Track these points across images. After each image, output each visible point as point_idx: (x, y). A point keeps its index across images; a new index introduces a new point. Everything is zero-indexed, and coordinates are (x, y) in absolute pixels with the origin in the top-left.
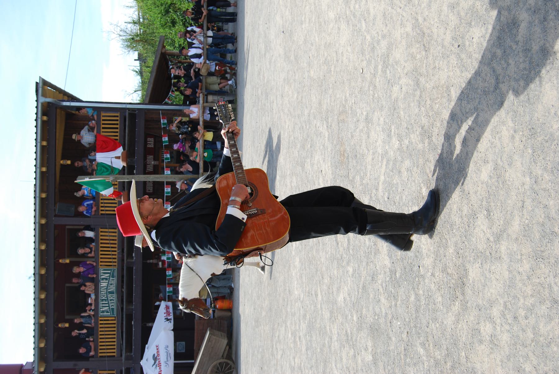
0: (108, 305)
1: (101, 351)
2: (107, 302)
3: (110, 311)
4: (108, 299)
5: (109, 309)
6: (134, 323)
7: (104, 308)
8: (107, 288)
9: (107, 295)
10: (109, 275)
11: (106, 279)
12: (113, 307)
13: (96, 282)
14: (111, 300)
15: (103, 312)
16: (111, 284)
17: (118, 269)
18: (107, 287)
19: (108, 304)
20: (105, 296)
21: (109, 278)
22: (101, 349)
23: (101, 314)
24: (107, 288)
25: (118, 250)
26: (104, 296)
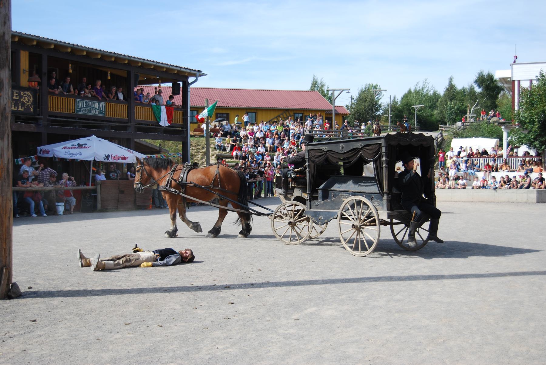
1: (59, 98)
3: (79, 108)
4: (86, 107)
5: (80, 108)
6: (71, 128)
7: (81, 103)
8: (93, 107)
9: (88, 107)
11: (99, 107)
13: (94, 98)
14: (86, 110)
15: (79, 102)
16: (96, 111)
19: (84, 108)
21: (99, 110)
22: (63, 98)
24: (93, 107)
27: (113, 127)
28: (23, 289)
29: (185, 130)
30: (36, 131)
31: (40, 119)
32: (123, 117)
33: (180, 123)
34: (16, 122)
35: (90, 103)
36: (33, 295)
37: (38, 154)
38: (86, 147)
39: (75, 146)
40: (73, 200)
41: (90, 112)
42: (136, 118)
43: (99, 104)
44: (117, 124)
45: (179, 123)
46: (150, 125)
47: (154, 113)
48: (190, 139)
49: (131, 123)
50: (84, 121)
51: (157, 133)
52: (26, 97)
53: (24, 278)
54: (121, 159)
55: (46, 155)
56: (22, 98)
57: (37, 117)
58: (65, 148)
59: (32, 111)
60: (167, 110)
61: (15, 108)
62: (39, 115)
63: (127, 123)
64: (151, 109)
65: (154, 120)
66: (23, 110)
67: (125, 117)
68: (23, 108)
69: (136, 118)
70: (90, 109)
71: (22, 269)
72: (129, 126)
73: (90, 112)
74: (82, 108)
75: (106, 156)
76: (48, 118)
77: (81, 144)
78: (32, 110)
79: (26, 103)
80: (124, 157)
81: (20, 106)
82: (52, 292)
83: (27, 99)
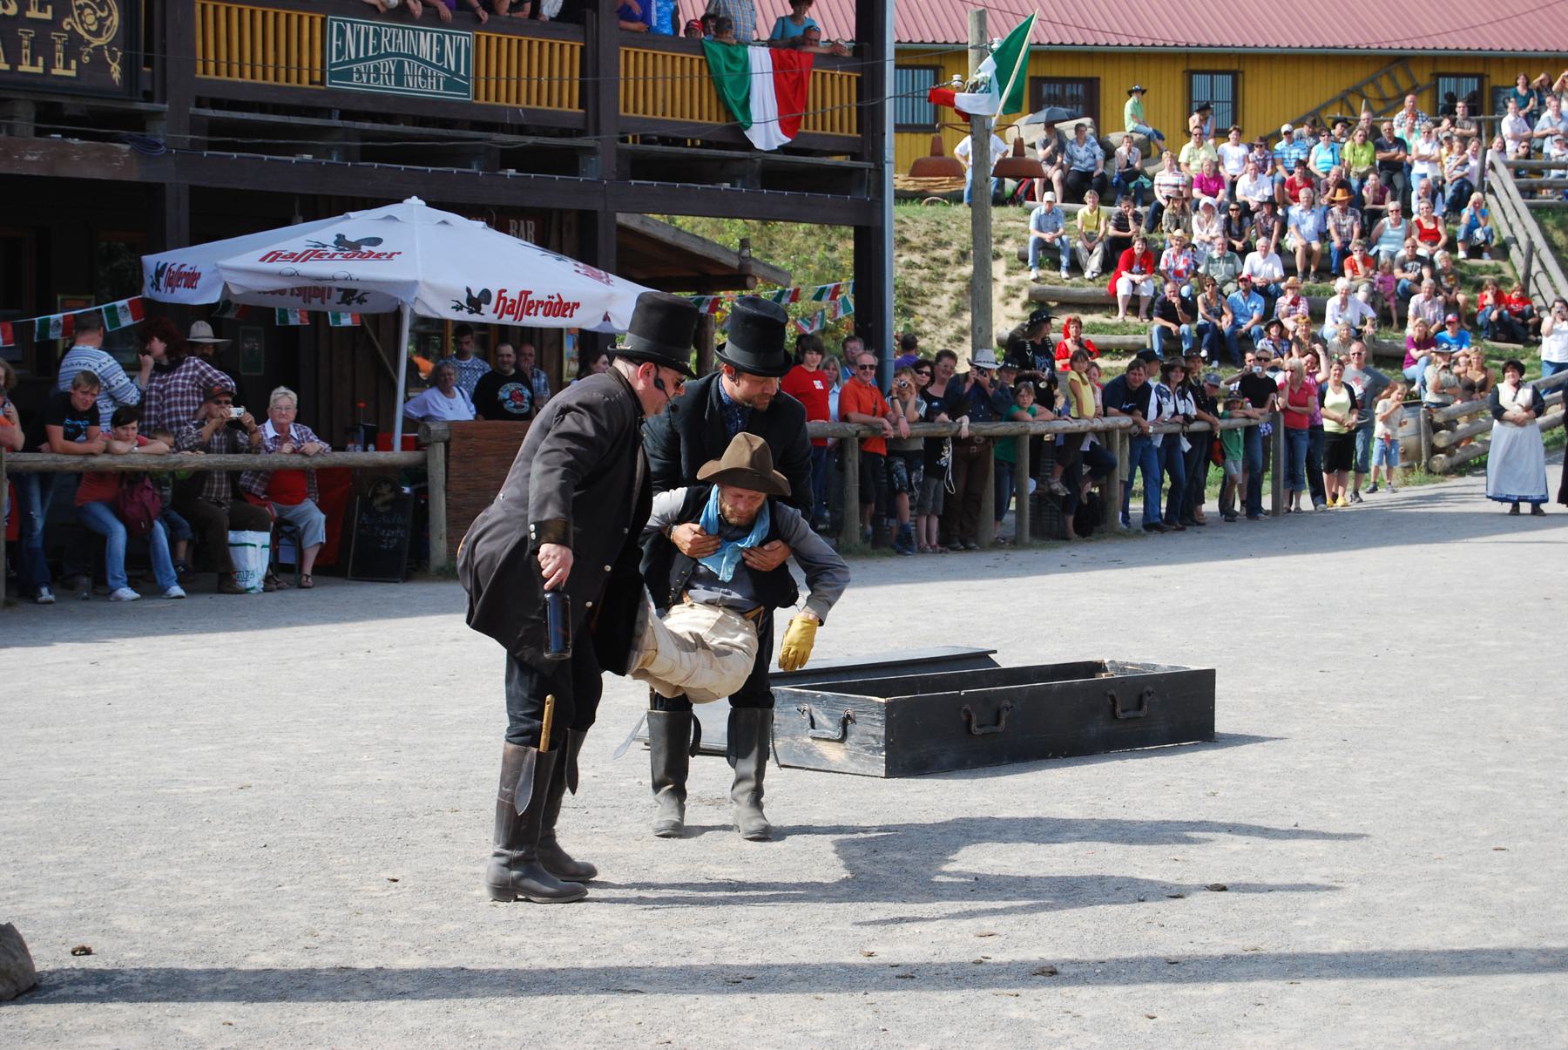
0: (362, 55)
2: (370, 54)
4: (380, 56)
5: (351, 62)
8: (413, 57)
9: (388, 55)
10: (453, 69)
11: (440, 57)
12: (355, 76)
14: (377, 69)
15: (342, 33)
16: (425, 76)
17: (470, 104)
18: (417, 58)
19: (367, 59)
20: (391, 46)
21: (441, 69)
22: (264, 14)
23: (335, 24)
24: (413, 57)
25: (525, 110)
26: (390, 42)
27: (509, 157)
28: (46, 957)
29: (872, 165)
30: (135, 175)
31: (157, 114)
32: (560, 104)
33: (846, 133)
34: (39, 132)
35: (396, 37)
36: (91, 990)
37: (148, 292)
38: (378, 256)
39: (324, 246)
40: (314, 521)
41: (399, 81)
42: (626, 110)
43: (441, 42)
44: (530, 140)
45: (837, 132)
46: (693, 145)
47: (717, 83)
48: (895, 214)
49: (597, 133)
50: (367, 125)
51: (727, 185)
52: (88, 11)
53: (55, 900)
54: (541, 310)
55: (183, 296)
56: (69, 13)
57: (143, 106)
58: (274, 256)
59: (116, 76)
60: (781, 67)
61: (34, 63)
62: (148, 97)
63: (580, 133)
64: (696, 63)
65: (714, 116)
66: (72, 73)
67: (567, 103)
68: (73, 64)
69: (626, 110)
70: (400, 66)
71: (52, 858)
72: (590, 151)
73: (399, 81)
74: (358, 60)
75: (470, 300)
76: (192, 110)
77: (352, 237)
78: (116, 71)
79: (86, 36)
80: (561, 301)
81: (60, 55)
82: (183, 972)
83: (90, 19)
